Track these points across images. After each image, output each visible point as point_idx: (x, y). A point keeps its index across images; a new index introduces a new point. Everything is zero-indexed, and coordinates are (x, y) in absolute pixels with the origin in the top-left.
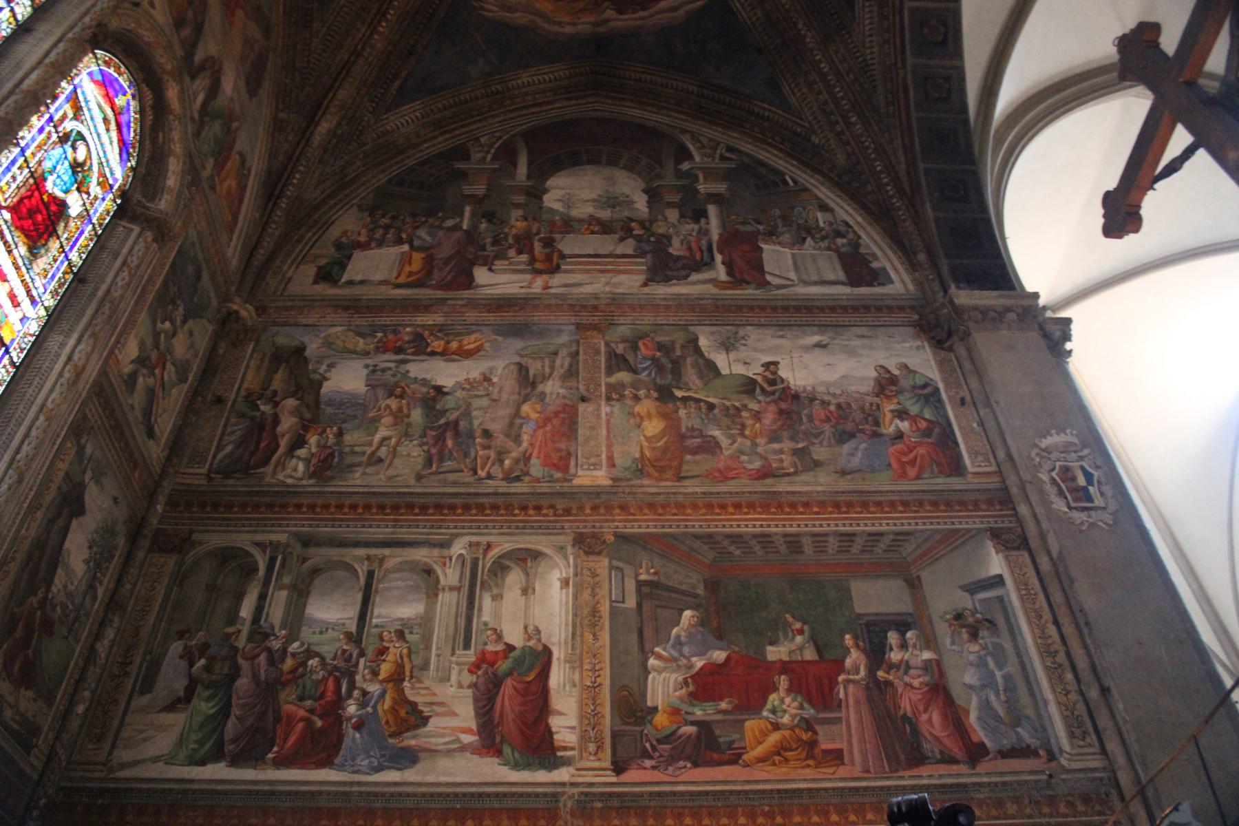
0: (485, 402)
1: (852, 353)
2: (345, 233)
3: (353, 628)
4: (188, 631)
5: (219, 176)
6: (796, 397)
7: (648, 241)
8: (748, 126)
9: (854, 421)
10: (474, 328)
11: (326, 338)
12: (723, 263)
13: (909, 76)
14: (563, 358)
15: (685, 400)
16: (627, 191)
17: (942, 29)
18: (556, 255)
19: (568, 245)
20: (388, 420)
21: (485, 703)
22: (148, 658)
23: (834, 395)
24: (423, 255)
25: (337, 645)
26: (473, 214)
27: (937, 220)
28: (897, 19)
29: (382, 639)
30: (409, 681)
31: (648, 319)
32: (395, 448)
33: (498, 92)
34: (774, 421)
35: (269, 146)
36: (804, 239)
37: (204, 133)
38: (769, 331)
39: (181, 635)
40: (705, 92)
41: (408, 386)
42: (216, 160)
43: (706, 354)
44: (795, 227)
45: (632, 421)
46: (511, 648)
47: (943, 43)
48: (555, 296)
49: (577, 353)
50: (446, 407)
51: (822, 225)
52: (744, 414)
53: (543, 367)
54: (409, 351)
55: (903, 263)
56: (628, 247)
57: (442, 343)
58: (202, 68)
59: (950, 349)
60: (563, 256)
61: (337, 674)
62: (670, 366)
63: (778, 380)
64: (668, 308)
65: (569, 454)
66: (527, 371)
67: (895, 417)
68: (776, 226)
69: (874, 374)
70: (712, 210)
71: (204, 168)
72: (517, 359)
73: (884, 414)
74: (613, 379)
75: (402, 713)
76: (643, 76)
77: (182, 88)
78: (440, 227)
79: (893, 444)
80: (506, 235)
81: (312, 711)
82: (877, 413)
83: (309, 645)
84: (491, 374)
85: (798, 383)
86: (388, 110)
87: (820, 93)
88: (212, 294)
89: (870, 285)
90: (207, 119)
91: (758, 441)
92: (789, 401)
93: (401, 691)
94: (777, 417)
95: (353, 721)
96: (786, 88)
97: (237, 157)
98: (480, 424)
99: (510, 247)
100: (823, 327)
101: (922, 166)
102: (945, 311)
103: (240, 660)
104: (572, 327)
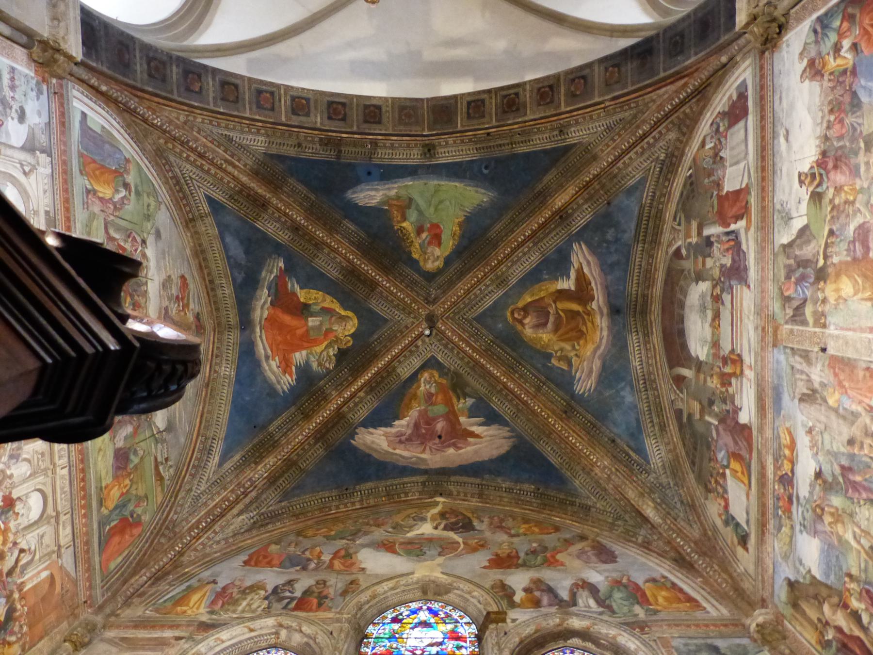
0: (826, 436)
1: (792, 106)
2: (720, 515)
5: (651, 605)
6: (824, 154)
7: (723, 283)
8: (661, 206)
9: (842, 96)
10: (776, 432)
11: (782, 558)
12: (736, 223)
13: (606, 98)
14: (796, 362)
15: (826, 257)
16: (697, 296)
17: (577, 80)
18: (732, 356)
19: (726, 348)
20: (840, 528)
23: (823, 118)
24: (732, 460)
26: (710, 415)
27: (696, 54)
28: (575, 113)
31: (771, 288)
32: (862, 531)
33: (645, 383)
34: (843, 173)
35: (655, 555)
36: (721, 158)
37: (615, 607)
38: (778, 184)
40: (641, 238)
41: (815, 501)
42: (638, 603)
43: (793, 237)
44: (715, 166)
45: (841, 306)
47: (584, 77)
48: (756, 361)
49: (792, 349)
50: (830, 472)
51: (712, 145)
52: (837, 201)
53: (802, 380)
54: (791, 491)
55: (733, 73)
56: (726, 298)
57: (785, 462)
58: (573, 595)
59: (786, 15)
60: (733, 351)
62: (801, 269)
63: (813, 171)
64: (763, 269)
65: (868, 369)
66: (804, 394)
67: (839, 55)
68: (713, 181)
69: (807, 81)
70: (707, 232)
71: (636, 615)
72: (796, 401)
73: (838, 66)
74: (810, 320)
76: (635, 282)
77: (577, 615)
78: (717, 441)
79: (862, 51)
80: (721, 392)
82: (837, 74)
84: (806, 426)
85: (813, 153)
86: (648, 462)
87: (630, 158)
88: (737, 641)
89: (746, 98)
90: (607, 602)
91: (858, 187)
92: (827, 159)
94: (839, 171)
96: (632, 182)
97: (647, 584)
98: (843, 446)
99: (727, 391)
100: (775, 135)
101: (662, 75)
102: (755, 29)
104: (775, 351)
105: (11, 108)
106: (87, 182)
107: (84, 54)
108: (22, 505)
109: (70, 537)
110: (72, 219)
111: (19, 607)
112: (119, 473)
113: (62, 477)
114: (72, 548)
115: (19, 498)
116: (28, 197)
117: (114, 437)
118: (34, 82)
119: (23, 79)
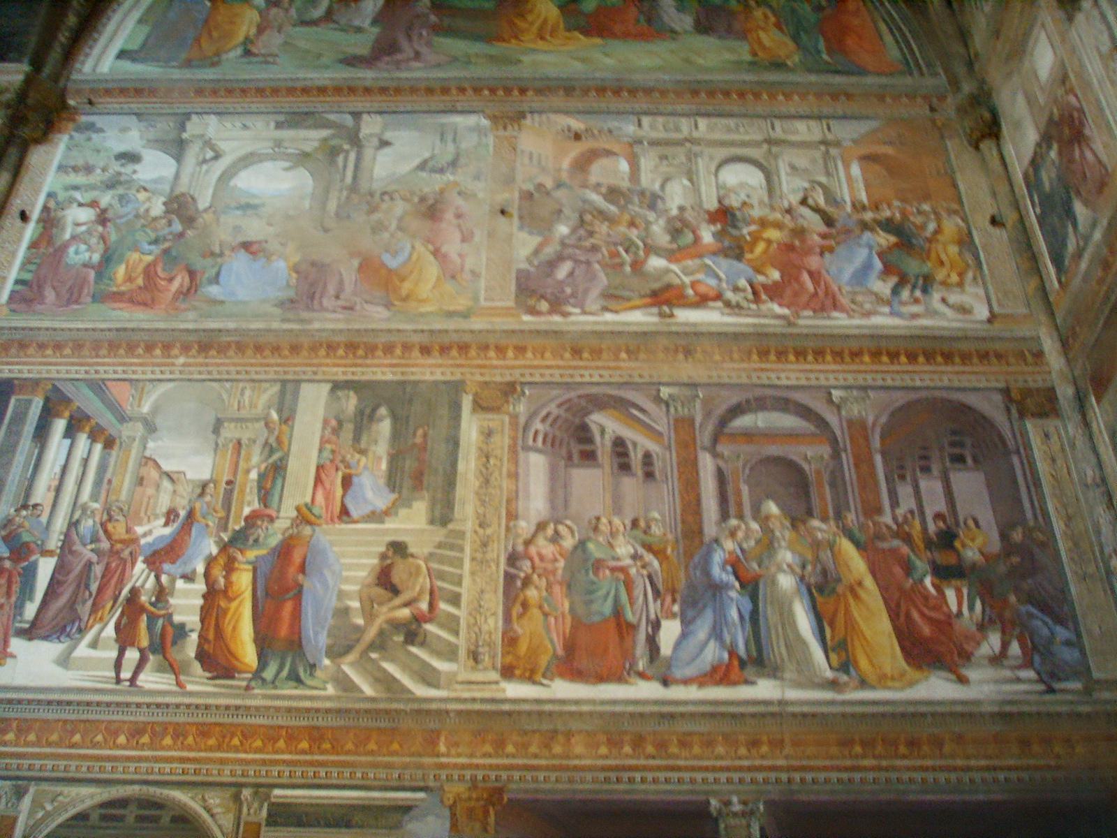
105: (119, 174)
106: (232, 55)
107: (19, 61)
108: (733, 196)
109: (812, 123)
110: (290, 84)
111: (888, 213)
112: (737, 26)
113: (711, 128)
114: (832, 123)
115: (720, 202)
116: (252, 154)
117: (673, 31)
118: (75, 134)
119: (75, 153)
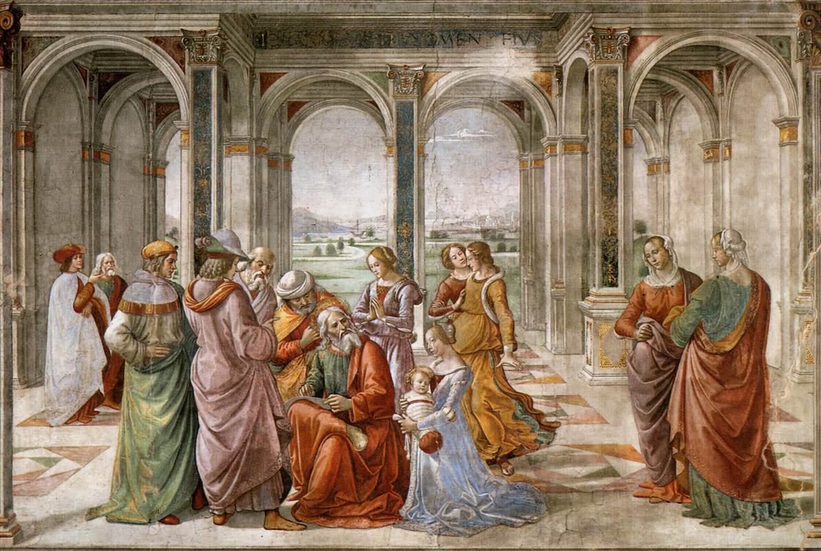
3: (386, 235)
4: (75, 251)
21: (650, 396)
22: (16, 311)
25: (368, 277)
29: (448, 264)
30: (512, 355)
39: (64, 259)
46: (690, 280)
61: (378, 340)
75: (507, 417)
81: (343, 416)
83: (313, 277)
93: (500, 374)
95: (423, 433)
103: (190, 315)
